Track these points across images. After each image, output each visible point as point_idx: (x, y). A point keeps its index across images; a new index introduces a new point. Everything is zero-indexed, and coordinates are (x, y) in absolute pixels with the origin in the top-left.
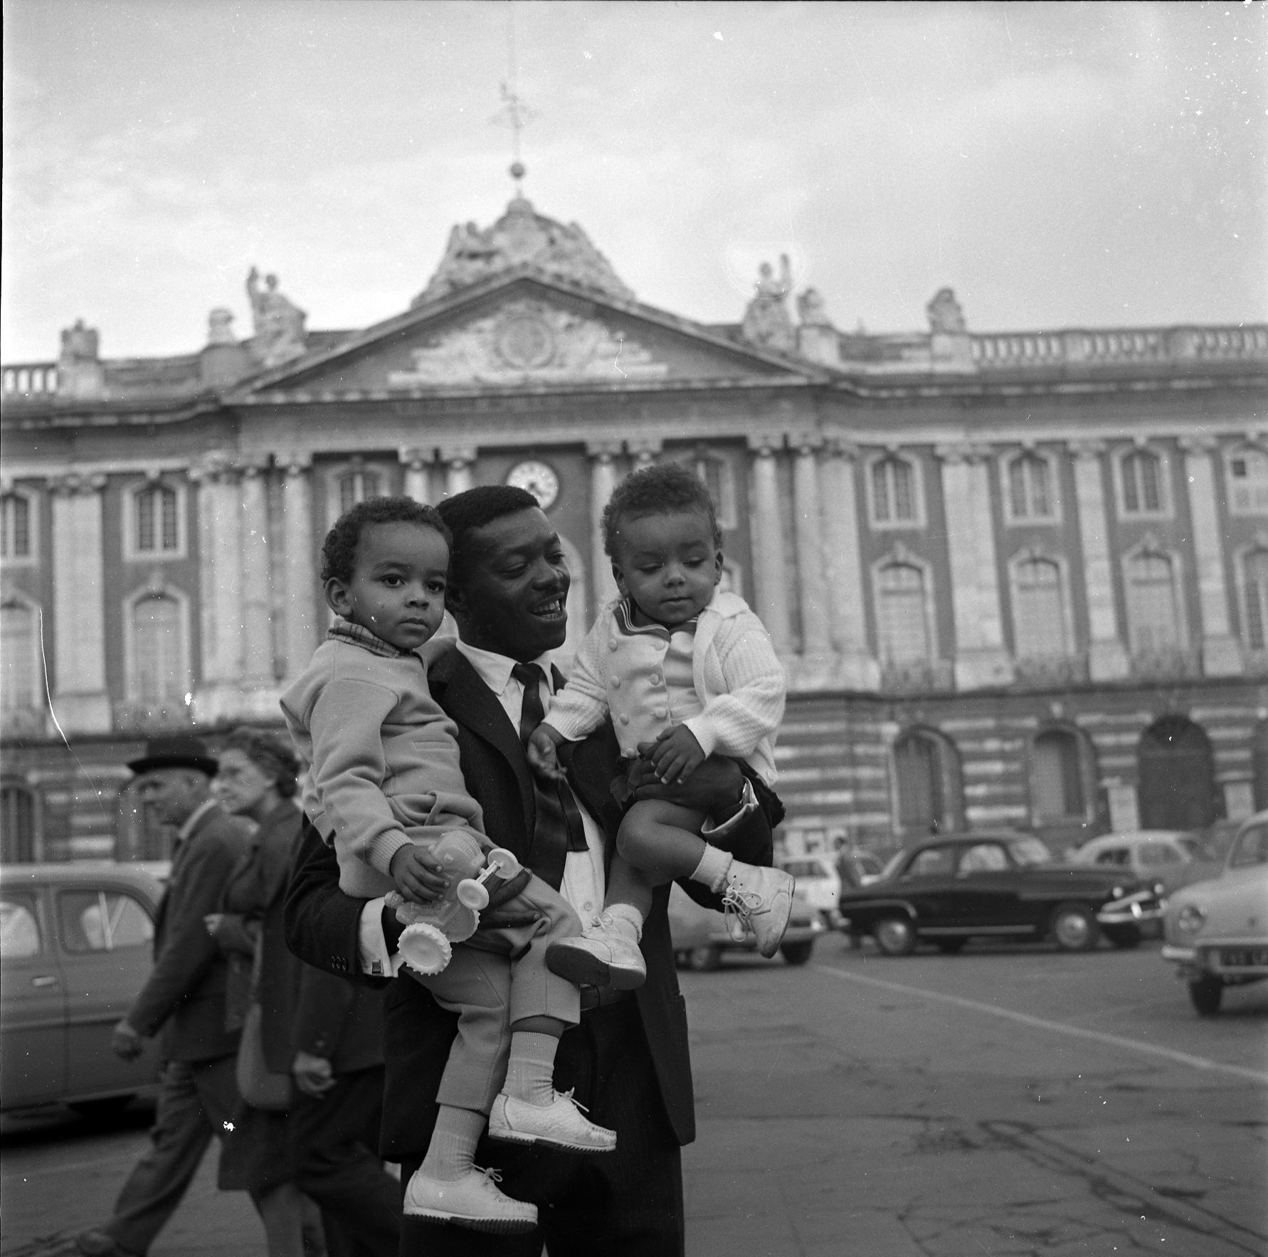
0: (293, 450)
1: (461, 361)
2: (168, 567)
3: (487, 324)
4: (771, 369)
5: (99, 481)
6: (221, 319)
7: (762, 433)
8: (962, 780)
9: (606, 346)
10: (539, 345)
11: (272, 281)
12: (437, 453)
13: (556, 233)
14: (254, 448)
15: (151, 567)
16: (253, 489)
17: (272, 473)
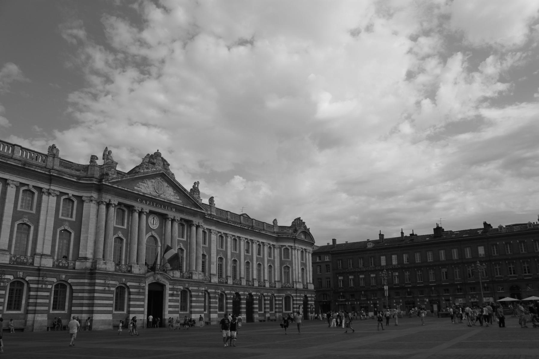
0: (115, 201)
1: (146, 188)
2: (69, 221)
3: (153, 181)
4: (197, 206)
5: (58, 194)
6: (93, 158)
7: (196, 221)
8: (210, 303)
9: (173, 193)
10: (161, 189)
11: (110, 152)
12: (142, 209)
13: (165, 163)
14: (106, 198)
15: (66, 220)
16: (103, 207)
17: (108, 205)
